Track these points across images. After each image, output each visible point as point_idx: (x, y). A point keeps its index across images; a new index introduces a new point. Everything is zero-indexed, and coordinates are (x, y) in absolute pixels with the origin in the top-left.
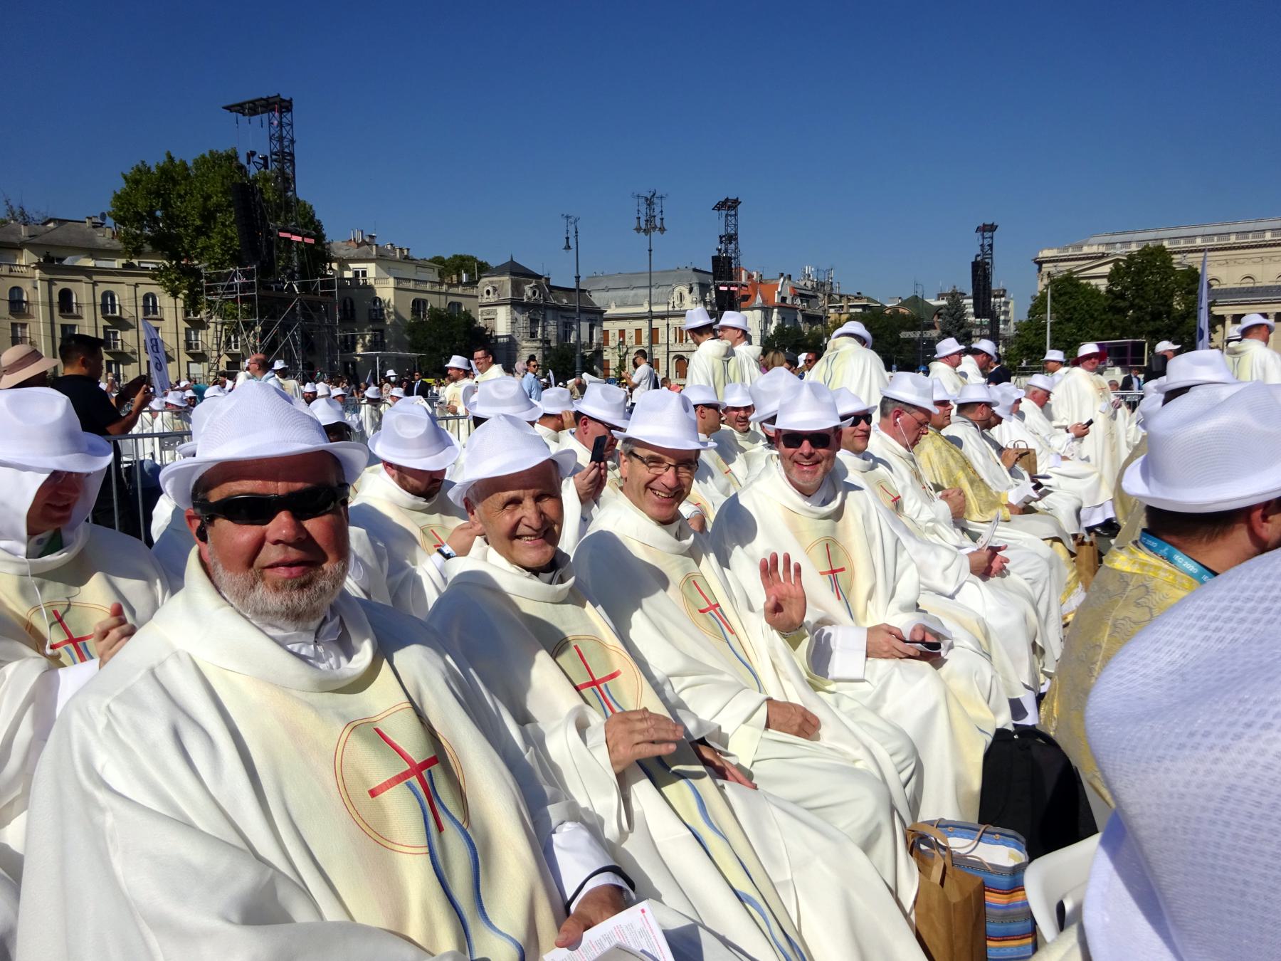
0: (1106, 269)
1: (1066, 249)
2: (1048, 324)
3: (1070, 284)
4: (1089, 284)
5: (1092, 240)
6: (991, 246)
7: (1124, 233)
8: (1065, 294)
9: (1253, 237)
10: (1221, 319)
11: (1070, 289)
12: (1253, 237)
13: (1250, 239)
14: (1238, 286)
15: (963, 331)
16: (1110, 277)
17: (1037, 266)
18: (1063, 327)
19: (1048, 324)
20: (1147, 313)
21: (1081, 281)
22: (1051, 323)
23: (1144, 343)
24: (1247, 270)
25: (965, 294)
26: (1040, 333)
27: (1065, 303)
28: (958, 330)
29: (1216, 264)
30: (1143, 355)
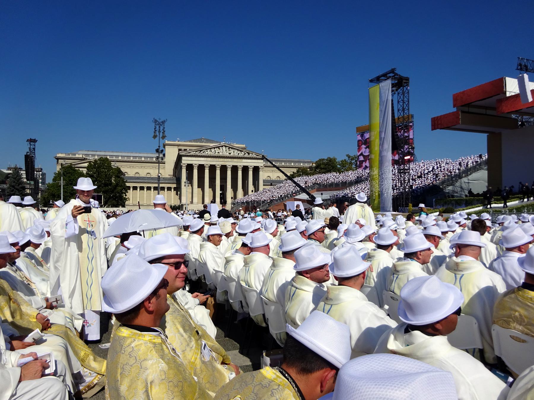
0: (86, 165)
1: (69, 154)
2: (62, 185)
3: (71, 169)
4: (79, 170)
5: (80, 152)
6: (34, 149)
7: (93, 151)
8: (69, 173)
9: (150, 159)
10: (129, 188)
11: (71, 171)
12: (150, 159)
13: (137, 159)
14: (134, 176)
15: (20, 186)
16: (87, 168)
17: (56, 160)
18: (69, 187)
19: (62, 185)
20: (102, 184)
21: (76, 169)
22: (63, 185)
23: (102, 195)
24: (137, 171)
25: (22, 169)
26: (59, 189)
27: (69, 177)
28: (18, 185)
29: (126, 167)
30: (102, 200)
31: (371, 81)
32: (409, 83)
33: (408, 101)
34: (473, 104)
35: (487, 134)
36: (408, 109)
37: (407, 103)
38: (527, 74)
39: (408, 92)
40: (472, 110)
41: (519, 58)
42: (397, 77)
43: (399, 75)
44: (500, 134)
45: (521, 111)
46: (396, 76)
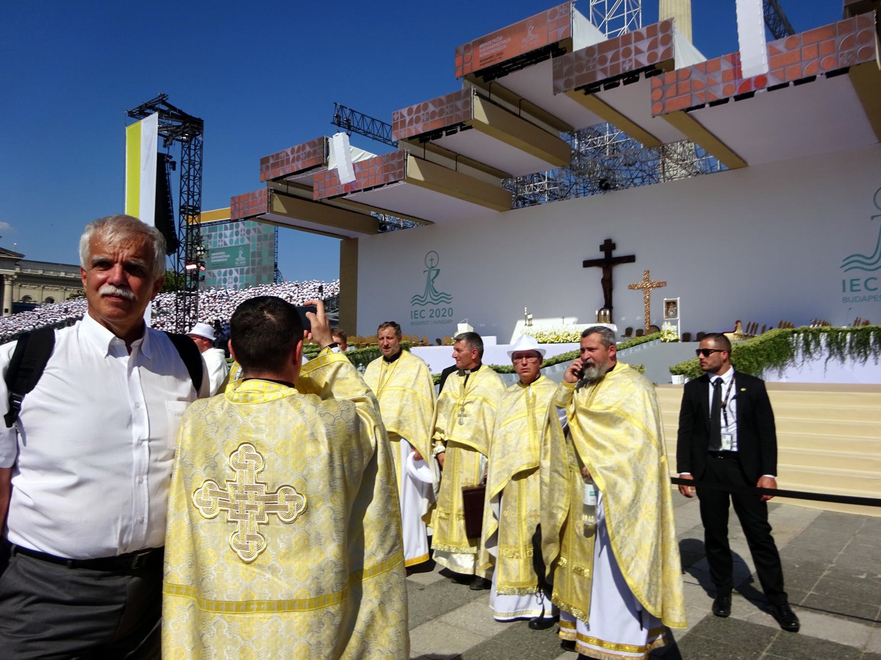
31: (131, 114)
32: (202, 129)
33: (201, 165)
34: (288, 179)
35: (339, 240)
36: (200, 178)
37: (197, 167)
38: (349, 135)
39: (201, 147)
40: (292, 190)
41: (336, 104)
42: (175, 113)
43: (180, 111)
44: (356, 240)
45: (344, 197)
46: (173, 112)
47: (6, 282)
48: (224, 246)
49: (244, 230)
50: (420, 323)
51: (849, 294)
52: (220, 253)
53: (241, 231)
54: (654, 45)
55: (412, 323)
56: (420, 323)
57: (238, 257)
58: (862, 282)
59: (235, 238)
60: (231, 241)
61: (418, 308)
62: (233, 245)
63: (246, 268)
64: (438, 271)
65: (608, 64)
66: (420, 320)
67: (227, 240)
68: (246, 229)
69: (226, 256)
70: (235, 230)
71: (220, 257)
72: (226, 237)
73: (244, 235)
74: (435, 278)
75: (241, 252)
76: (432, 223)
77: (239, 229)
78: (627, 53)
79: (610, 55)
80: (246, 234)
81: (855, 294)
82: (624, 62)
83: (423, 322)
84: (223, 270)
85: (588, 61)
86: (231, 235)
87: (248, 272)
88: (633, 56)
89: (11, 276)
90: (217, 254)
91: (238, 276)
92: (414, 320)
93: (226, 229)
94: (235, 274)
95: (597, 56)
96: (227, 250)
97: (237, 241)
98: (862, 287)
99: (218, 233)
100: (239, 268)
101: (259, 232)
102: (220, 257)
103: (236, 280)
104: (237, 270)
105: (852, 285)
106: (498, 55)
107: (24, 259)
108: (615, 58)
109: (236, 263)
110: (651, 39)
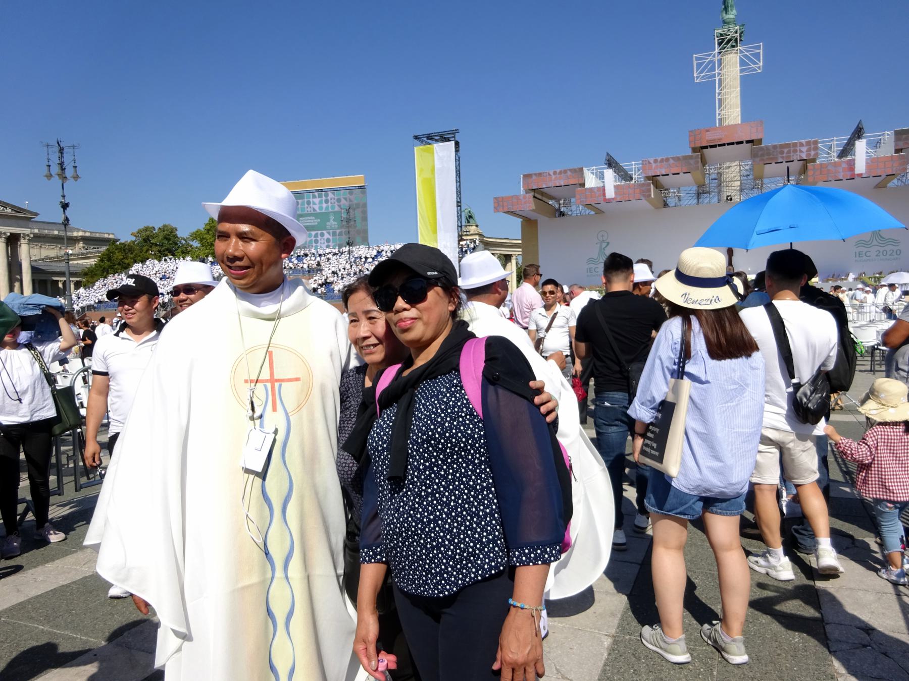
31: (416, 137)
47: (22, 241)
48: (312, 212)
49: (334, 199)
50: (594, 276)
51: (858, 258)
52: (310, 218)
53: (331, 199)
54: (809, 150)
55: (588, 276)
56: (594, 276)
57: (329, 221)
58: (864, 253)
59: (324, 205)
60: (321, 208)
61: (593, 266)
62: (323, 211)
63: (338, 231)
64: (608, 243)
65: (785, 155)
66: (594, 273)
67: (316, 207)
68: (336, 198)
69: (316, 221)
70: (324, 198)
71: (309, 221)
72: (314, 204)
73: (335, 203)
74: (606, 247)
75: (332, 218)
76: (603, 212)
77: (329, 198)
78: (795, 151)
79: (786, 150)
80: (336, 203)
81: (861, 258)
82: (793, 155)
83: (597, 275)
84: (313, 233)
85: (774, 152)
86: (320, 203)
87: (340, 234)
88: (798, 153)
89: (28, 235)
90: (307, 218)
91: (331, 238)
92: (589, 274)
93: (314, 197)
94: (326, 236)
95: (778, 150)
96: (316, 215)
97: (327, 208)
98: (864, 255)
99: (306, 200)
100: (331, 231)
101: (350, 201)
102: (309, 221)
103: (328, 240)
104: (329, 233)
105: (859, 254)
106: (719, 139)
107: (37, 219)
108: (789, 152)
109: (328, 227)
110: (807, 147)
